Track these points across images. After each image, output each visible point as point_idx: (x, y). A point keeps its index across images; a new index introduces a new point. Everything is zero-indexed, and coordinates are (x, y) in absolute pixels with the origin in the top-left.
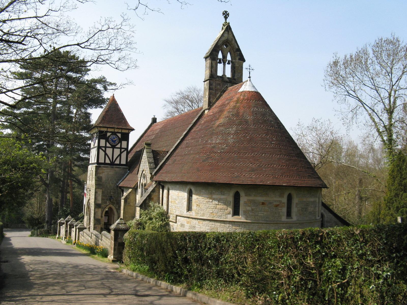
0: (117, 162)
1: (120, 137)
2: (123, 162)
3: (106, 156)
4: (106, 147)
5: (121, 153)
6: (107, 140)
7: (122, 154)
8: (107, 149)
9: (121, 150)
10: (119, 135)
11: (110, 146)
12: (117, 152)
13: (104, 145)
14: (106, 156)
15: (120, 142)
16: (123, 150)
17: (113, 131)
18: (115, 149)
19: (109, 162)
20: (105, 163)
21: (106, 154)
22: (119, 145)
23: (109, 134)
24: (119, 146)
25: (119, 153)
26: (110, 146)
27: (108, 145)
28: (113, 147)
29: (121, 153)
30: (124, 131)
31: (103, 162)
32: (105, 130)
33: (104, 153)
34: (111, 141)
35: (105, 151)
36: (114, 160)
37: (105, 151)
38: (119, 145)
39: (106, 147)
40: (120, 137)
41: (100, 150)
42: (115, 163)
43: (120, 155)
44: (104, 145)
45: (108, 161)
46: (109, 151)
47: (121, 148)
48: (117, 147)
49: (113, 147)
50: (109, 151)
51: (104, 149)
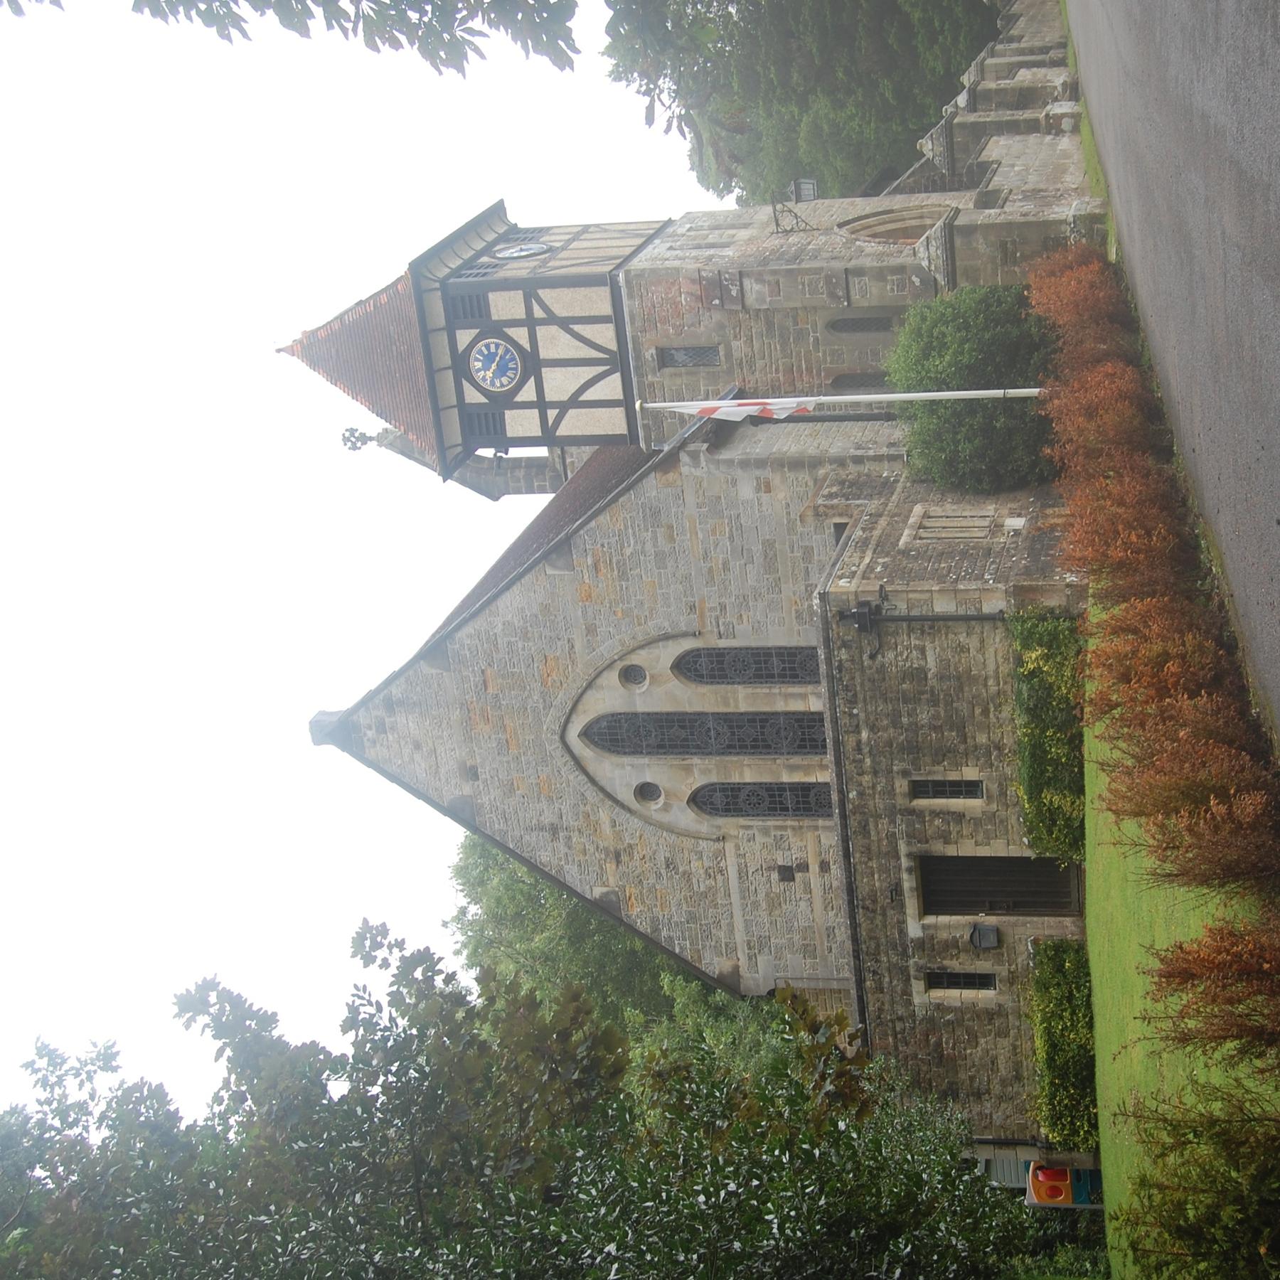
0: (605, 335)
1: (475, 332)
2: (600, 302)
3: (589, 395)
4: (541, 404)
5: (551, 319)
6: (506, 400)
7: (560, 311)
8: (550, 396)
9: (543, 322)
10: (464, 337)
11: (531, 382)
12: (554, 343)
13: (535, 413)
14: (589, 395)
15: (497, 330)
16: (538, 313)
17: (450, 372)
18: (544, 354)
19: (616, 378)
20: (627, 403)
21: (575, 402)
22: (512, 332)
23: (473, 396)
24: (521, 335)
25: (554, 329)
26: (531, 382)
27: (528, 393)
28: (532, 364)
29: (551, 319)
30: (438, 315)
31: (619, 413)
32: (453, 421)
33: (572, 413)
34: (505, 380)
35: (564, 407)
36: (602, 355)
37: (564, 407)
38: (512, 332)
39: (541, 404)
40: (475, 332)
41: (562, 431)
42: (613, 346)
43: (565, 324)
44: (535, 413)
45: (611, 387)
46: (559, 384)
47: (530, 323)
48: (527, 346)
49: (532, 364)
50: (559, 384)
51: (552, 414)
